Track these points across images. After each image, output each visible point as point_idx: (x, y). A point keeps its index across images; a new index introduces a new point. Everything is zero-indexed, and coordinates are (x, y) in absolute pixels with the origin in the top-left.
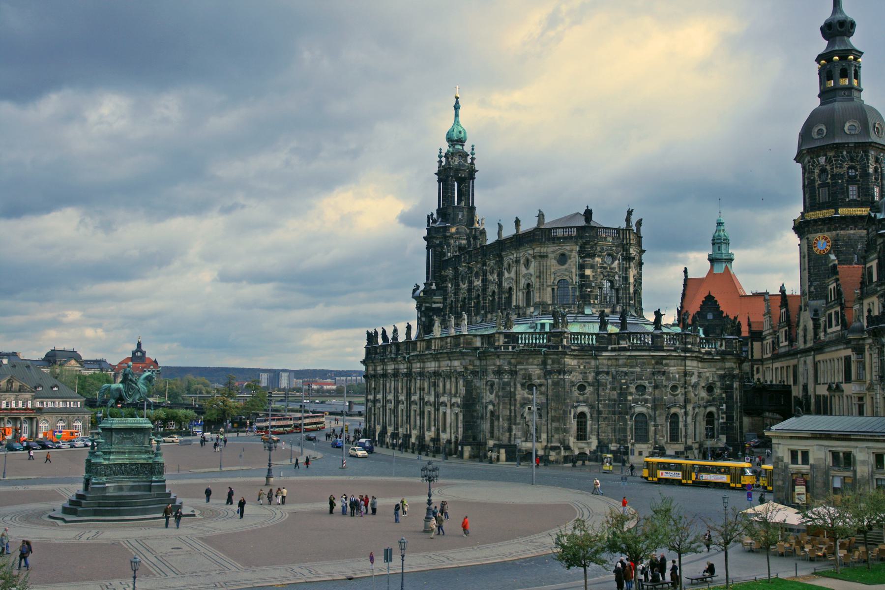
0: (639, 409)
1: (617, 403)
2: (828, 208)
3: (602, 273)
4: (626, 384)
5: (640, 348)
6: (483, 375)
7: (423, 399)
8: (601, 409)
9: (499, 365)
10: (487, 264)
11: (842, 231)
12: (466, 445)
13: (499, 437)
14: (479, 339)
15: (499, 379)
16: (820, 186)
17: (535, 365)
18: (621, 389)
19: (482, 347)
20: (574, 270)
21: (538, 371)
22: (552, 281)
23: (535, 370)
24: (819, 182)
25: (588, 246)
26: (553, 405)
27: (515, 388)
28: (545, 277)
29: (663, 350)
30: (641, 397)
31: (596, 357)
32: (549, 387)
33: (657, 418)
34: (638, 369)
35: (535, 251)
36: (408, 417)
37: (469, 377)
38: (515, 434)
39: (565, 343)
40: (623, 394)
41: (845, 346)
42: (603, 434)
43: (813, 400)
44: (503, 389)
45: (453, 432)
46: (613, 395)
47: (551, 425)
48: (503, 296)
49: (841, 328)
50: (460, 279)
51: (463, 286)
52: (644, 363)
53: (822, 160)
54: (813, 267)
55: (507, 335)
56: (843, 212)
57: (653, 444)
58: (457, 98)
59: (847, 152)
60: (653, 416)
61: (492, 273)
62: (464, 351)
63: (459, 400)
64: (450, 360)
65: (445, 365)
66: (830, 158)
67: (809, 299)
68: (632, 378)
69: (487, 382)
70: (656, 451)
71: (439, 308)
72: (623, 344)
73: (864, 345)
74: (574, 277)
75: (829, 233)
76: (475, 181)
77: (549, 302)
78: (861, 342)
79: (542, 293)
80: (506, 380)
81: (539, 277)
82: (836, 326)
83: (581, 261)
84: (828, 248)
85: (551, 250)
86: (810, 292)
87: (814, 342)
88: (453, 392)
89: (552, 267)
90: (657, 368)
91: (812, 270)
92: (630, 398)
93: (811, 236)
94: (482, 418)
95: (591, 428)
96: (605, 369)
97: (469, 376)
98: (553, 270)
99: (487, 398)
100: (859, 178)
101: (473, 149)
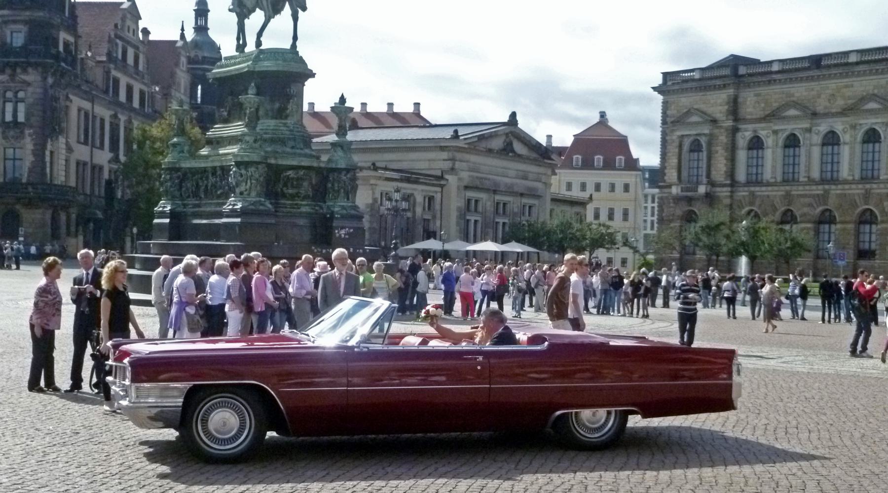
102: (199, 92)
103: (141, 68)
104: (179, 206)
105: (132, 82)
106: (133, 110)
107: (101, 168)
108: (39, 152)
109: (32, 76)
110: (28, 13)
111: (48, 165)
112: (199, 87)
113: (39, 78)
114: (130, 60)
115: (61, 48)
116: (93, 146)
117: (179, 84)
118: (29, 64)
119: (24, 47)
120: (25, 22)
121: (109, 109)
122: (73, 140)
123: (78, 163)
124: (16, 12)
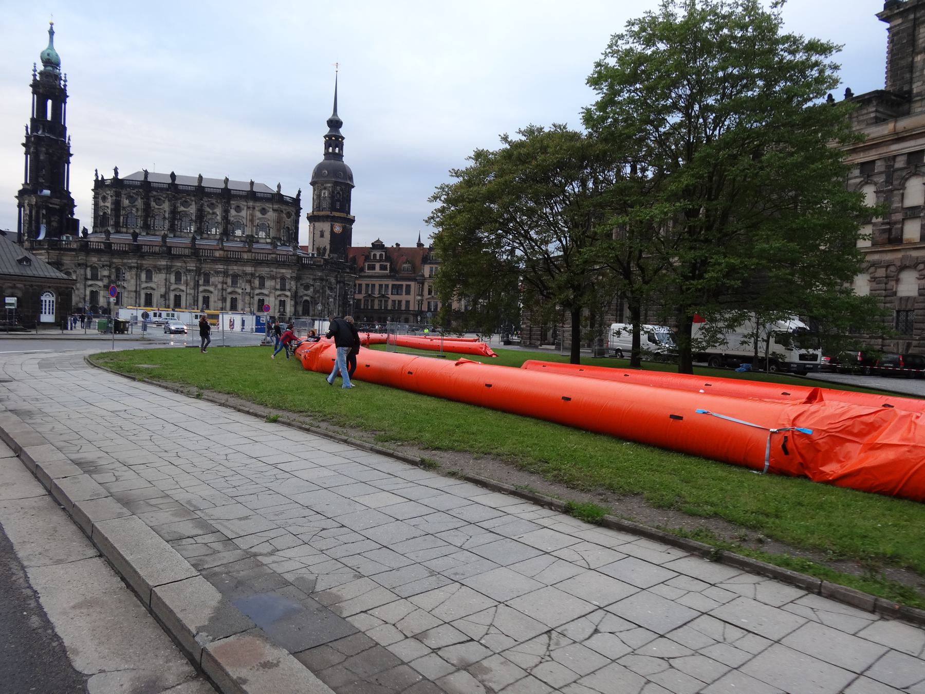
2: (340, 212)
7: (226, 290)
10: (205, 199)
23: (333, 280)
34: (351, 283)
35: (274, 206)
36: (196, 301)
44: (322, 289)
45: (277, 311)
50: (152, 199)
51: (157, 207)
53: (338, 188)
58: (52, 24)
61: (212, 206)
64: (276, 268)
65: (264, 271)
71: (55, 208)
76: (67, 105)
82: (380, 270)
88: (278, 287)
93: (332, 223)
97: (298, 279)
101: (65, 77)
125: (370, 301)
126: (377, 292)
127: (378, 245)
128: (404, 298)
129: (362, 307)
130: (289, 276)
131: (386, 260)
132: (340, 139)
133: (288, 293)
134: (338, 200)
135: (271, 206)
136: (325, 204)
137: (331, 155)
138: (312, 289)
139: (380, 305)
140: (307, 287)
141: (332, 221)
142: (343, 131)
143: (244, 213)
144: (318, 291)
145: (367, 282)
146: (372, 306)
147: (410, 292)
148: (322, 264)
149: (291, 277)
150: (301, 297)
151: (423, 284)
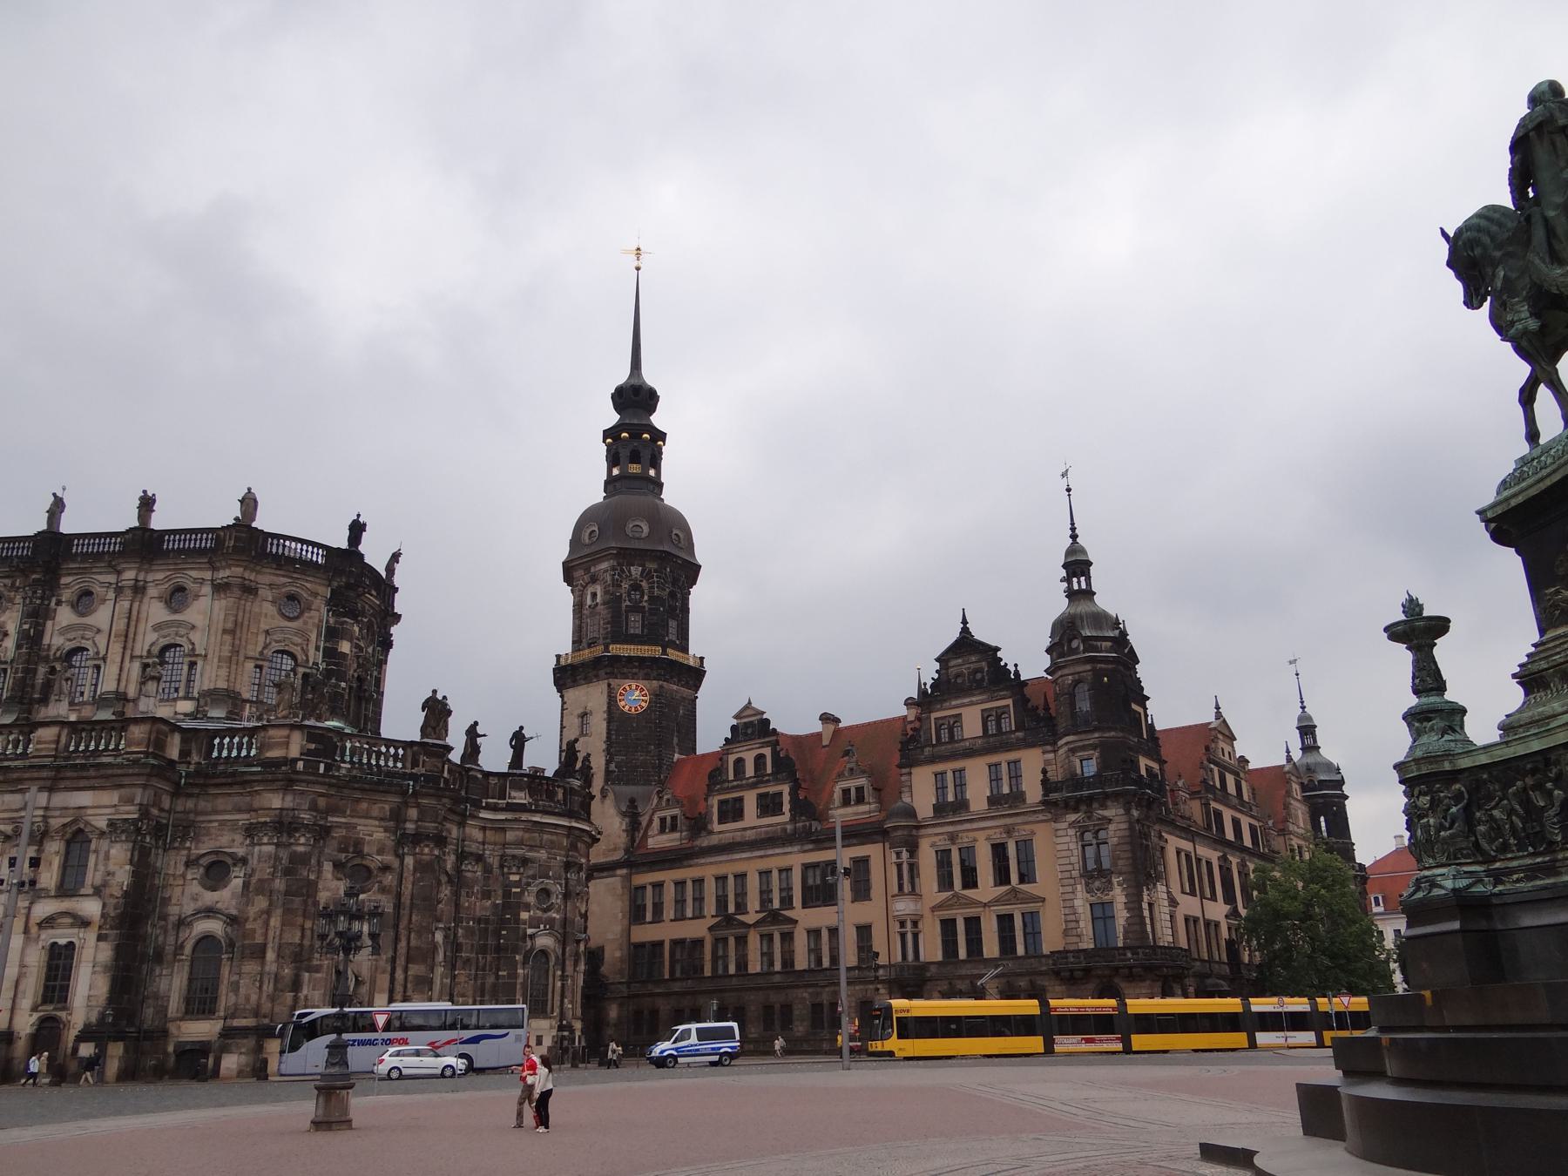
0: (545, 941)
1: (491, 928)
3: (358, 657)
4: (517, 884)
5: (550, 809)
6: (184, 840)
8: (461, 940)
9: (280, 809)
11: (665, 683)
12: (116, 1039)
13: (259, 1005)
14: (176, 739)
15: (277, 845)
16: (630, 610)
17: (375, 818)
18: (507, 894)
19: (189, 763)
20: (313, 637)
21: (379, 835)
22: (259, 649)
23: (373, 833)
24: (628, 603)
25: (352, 594)
26: (414, 918)
27: (319, 872)
28: (244, 636)
29: (578, 819)
30: (545, 915)
31: (462, 824)
32: (405, 875)
33: (567, 962)
34: (542, 855)
35: (223, 574)
37: (148, 840)
38: (306, 996)
39: (446, 775)
40: (512, 905)
41: (810, 846)
42: (460, 999)
43: (613, 954)
44: (288, 872)
45: (26, 1003)
46: (485, 909)
47: (406, 970)
48: (42, 670)
49: (793, 820)
52: (552, 842)
54: (616, 731)
55: (313, 735)
56: (673, 654)
57: (558, 1018)
59: (671, 571)
60: (560, 957)
62: (152, 761)
63: (91, 908)
64: (51, 790)
66: (650, 571)
67: (606, 781)
68: (531, 872)
69: (189, 864)
70: (566, 1033)
72: (520, 797)
73: (918, 837)
74: (312, 652)
75: (647, 682)
77: (246, 696)
78: (914, 832)
79: (233, 672)
80: (301, 849)
81: (232, 632)
83: (332, 621)
84: (643, 704)
85: (265, 578)
86: (608, 772)
87: (627, 851)
88: (49, 877)
89: (263, 619)
90: (572, 856)
91: (614, 737)
92: (524, 915)
93: (614, 682)
94: (159, 957)
95: (442, 983)
96: (473, 848)
98: (267, 628)
99: (185, 900)
100: (678, 611)
102: (1323, 824)
103: (1246, 797)
104: (1480, 881)
105: (1238, 815)
106: (1244, 849)
107: (1217, 924)
108: (1134, 904)
109: (1113, 812)
110: (1096, 735)
111: (1148, 921)
112: (1322, 819)
113: (1121, 811)
114: (1231, 789)
115: (1143, 772)
116: (1203, 897)
117: (1297, 817)
118: (1107, 796)
119: (1098, 775)
120: (1094, 747)
121: (1215, 850)
122: (1175, 889)
123: (1187, 919)
124: (1083, 736)
125: (732, 941)
126: (753, 903)
127: (751, 727)
128: (847, 913)
129: (708, 972)
130: (102, 823)
131: (778, 781)
132: (645, 435)
133: (91, 908)
134: (635, 608)
135: (208, 575)
136: (596, 628)
137: (618, 485)
138: (237, 883)
139: (768, 956)
140: (216, 872)
141: (612, 675)
142: (658, 420)
143: (101, 617)
144: (263, 888)
145: (721, 870)
146: (742, 964)
147: (868, 889)
148: (294, 752)
149: (112, 824)
150: (182, 923)
151: (913, 849)
